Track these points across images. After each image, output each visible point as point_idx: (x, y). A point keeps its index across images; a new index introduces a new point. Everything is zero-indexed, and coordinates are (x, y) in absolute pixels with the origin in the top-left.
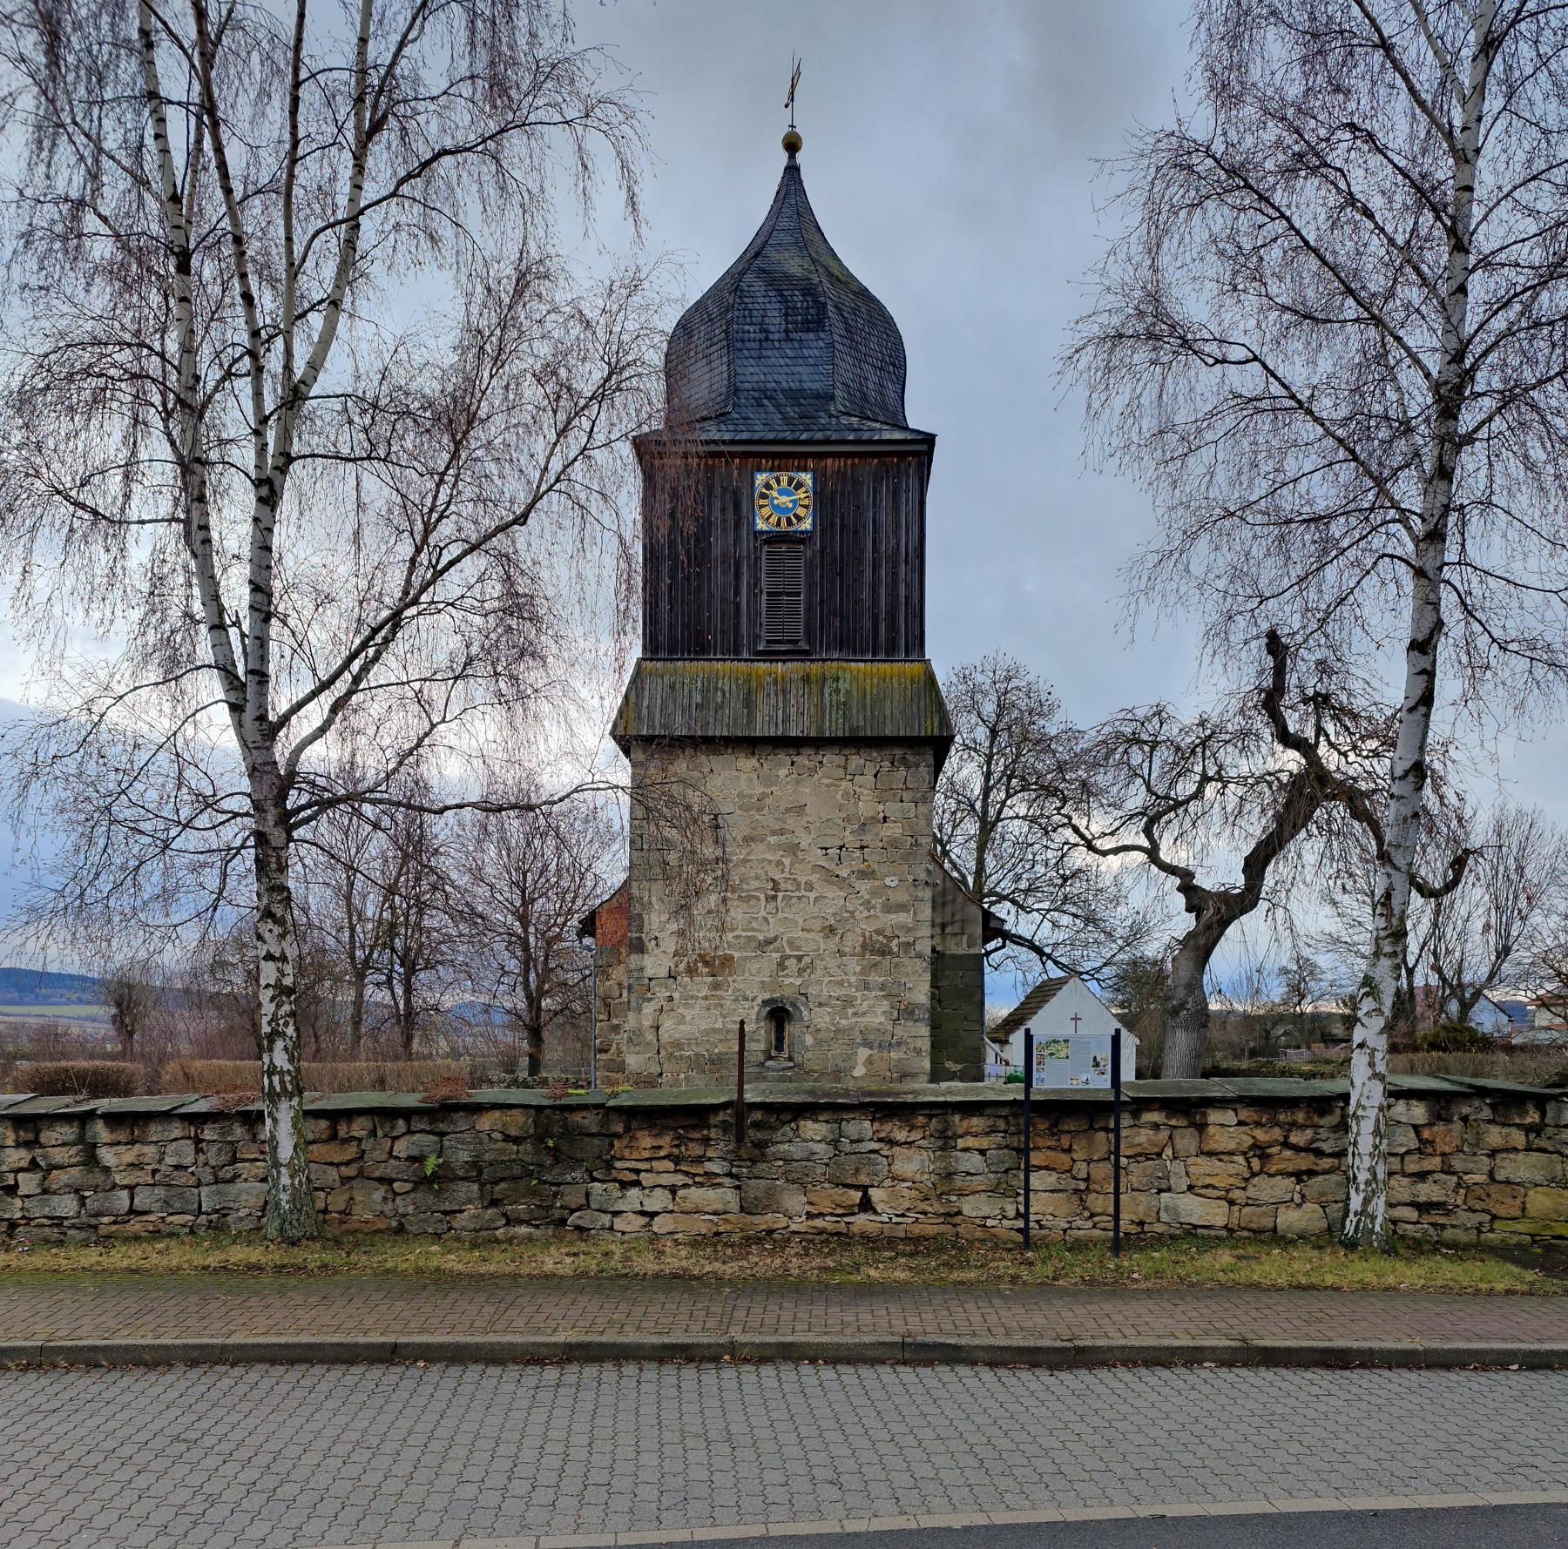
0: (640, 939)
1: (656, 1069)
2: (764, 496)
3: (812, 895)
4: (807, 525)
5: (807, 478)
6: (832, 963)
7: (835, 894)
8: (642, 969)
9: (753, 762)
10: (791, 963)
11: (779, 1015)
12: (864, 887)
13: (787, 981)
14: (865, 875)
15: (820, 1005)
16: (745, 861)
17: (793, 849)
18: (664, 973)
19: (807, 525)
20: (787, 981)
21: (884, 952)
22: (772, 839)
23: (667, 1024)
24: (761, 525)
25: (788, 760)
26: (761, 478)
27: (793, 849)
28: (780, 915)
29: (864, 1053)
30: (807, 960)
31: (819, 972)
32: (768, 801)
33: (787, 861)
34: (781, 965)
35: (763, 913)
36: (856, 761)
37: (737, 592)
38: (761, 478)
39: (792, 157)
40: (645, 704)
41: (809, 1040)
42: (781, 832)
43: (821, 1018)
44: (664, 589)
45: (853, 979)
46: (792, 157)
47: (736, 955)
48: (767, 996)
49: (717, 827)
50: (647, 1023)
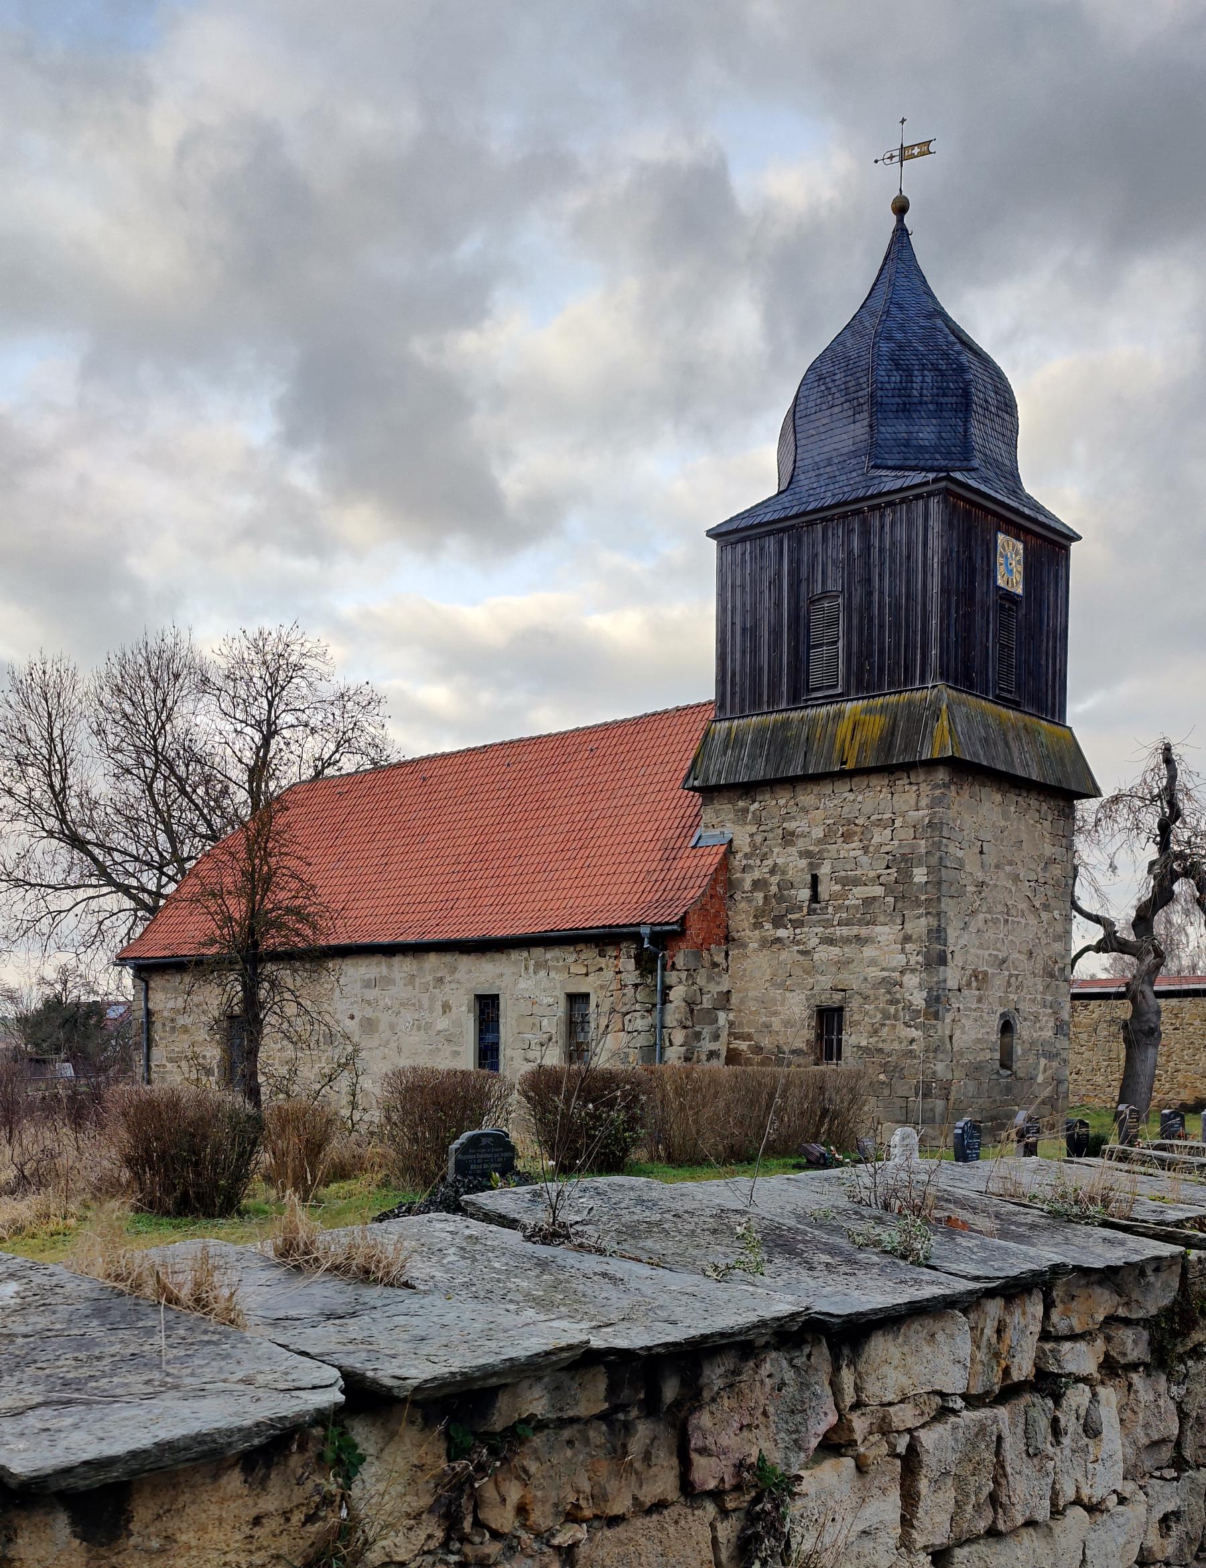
0: (944, 951)
1: (950, 1077)
2: (1002, 556)
3: (1023, 921)
4: (1019, 590)
5: (1020, 546)
6: (1030, 981)
7: (1032, 921)
8: (945, 981)
9: (998, 797)
10: (1013, 980)
11: (1007, 1027)
12: (1045, 916)
13: (1012, 996)
14: (1046, 907)
15: (1025, 1019)
16: (996, 886)
17: (1016, 878)
18: (956, 987)
19: (1019, 590)
20: (1012, 996)
21: (1052, 976)
22: (1008, 868)
23: (957, 1034)
24: (1000, 582)
25: (1015, 798)
26: (1001, 537)
27: (1016, 878)
28: (1010, 937)
29: (1043, 1061)
30: (1020, 979)
31: (1025, 990)
32: (1006, 833)
33: (1013, 889)
34: (1009, 984)
35: (1001, 936)
36: (1044, 807)
37: (987, 640)
38: (1001, 537)
39: (900, 220)
40: (959, 729)
41: (1020, 1052)
42: (1011, 863)
43: (1023, 1030)
44: (953, 622)
45: (1039, 997)
46: (900, 220)
47: (990, 971)
48: (1001, 1010)
49: (981, 852)
50: (948, 1033)
